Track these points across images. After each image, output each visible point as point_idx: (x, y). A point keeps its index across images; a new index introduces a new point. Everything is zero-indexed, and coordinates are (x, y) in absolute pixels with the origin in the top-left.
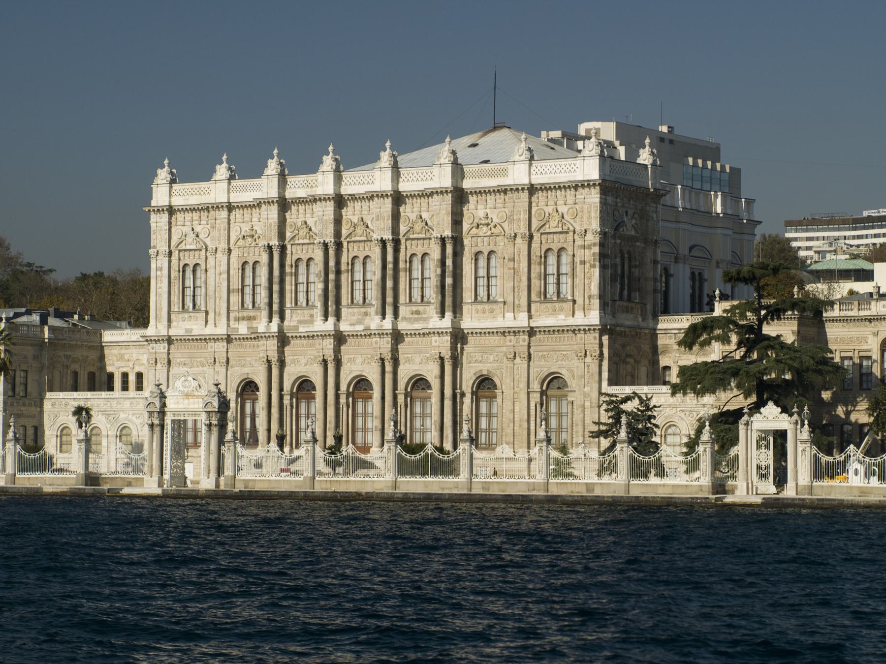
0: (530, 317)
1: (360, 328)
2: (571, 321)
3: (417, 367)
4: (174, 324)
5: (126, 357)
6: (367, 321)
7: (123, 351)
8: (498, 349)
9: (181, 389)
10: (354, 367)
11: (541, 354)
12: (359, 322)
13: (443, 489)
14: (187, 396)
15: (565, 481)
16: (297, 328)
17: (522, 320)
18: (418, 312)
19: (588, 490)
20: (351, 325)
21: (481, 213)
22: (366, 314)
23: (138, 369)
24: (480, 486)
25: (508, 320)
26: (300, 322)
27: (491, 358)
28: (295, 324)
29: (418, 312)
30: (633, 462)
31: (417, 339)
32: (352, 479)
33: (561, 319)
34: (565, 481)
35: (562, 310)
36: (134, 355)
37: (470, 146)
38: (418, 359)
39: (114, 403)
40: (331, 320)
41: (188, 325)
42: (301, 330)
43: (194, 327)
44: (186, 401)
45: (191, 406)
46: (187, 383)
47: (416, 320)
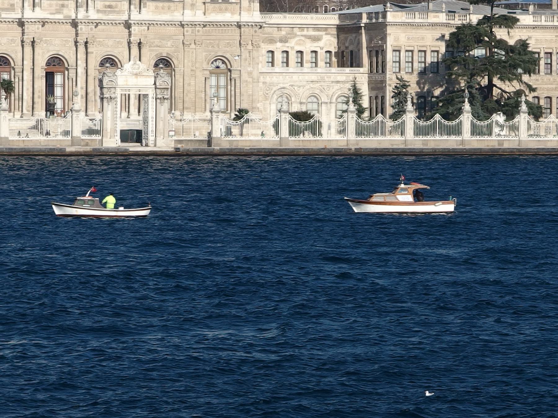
1: (60, 16)
2: (236, 18)
3: (109, 49)
6: (65, 11)
8: (175, 37)
9: (130, 70)
10: (51, 48)
11: (208, 41)
12: (58, 12)
13: (392, 145)
15: (481, 138)
17: (199, 17)
19: (499, 145)
20: (51, 14)
22: (63, 6)
24: (421, 142)
25: (189, 16)
27: (169, 44)
29: (110, 7)
30: (473, 125)
31: (110, 27)
32: (318, 138)
34: (481, 138)
35: (226, 9)
38: (110, 42)
40: (37, 9)
46: (137, 67)
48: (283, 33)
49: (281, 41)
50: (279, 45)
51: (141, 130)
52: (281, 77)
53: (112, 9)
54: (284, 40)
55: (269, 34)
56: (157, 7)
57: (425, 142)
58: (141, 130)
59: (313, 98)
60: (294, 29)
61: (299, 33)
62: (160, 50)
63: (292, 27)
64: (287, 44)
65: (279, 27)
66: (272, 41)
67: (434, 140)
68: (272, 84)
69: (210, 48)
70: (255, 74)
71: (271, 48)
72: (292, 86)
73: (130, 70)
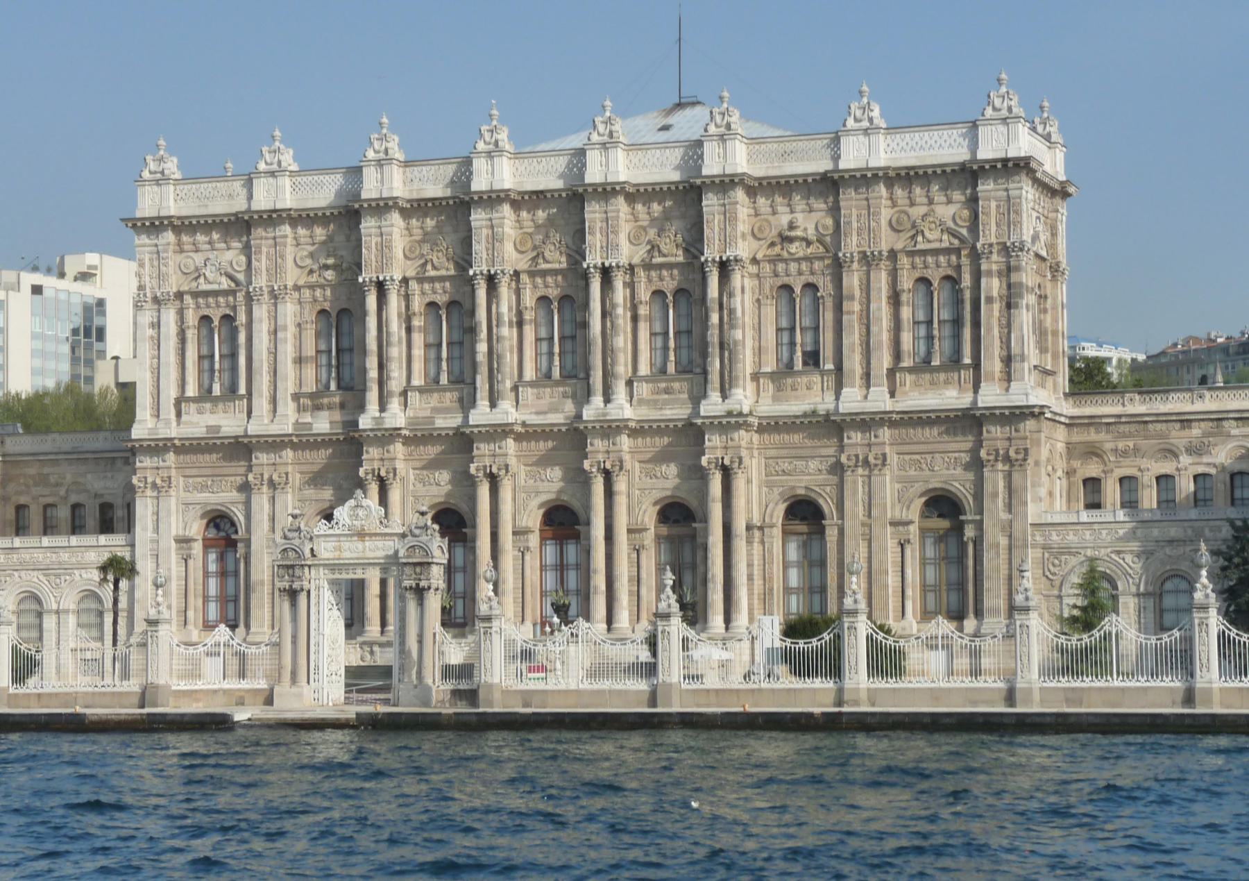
0: (892, 394)
4: (184, 418)
5: (52, 480)
7: (46, 470)
12: (554, 409)
14: (362, 535)
16: (430, 420)
17: (879, 400)
18: (667, 391)
20: (538, 413)
21: (785, 220)
23: (74, 498)
26: (435, 410)
28: (428, 413)
33: (952, 397)
35: (947, 382)
36: (69, 477)
37: (660, 129)
39: (65, 556)
40: (506, 405)
41: (210, 419)
42: (440, 422)
43: (223, 423)
44: (360, 545)
45: (369, 554)
46: (361, 512)
47: (666, 403)
48: (1196, 431)
49: (1190, 451)
50: (1185, 460)
51: (391, 667)
52: (1088, 533)
53: (673, 397)
54: (1195, 450)
55: (1161, 436)
56: (779, 389)
57: (1073, 695)
58: (391, 667)
59: (1176, 581)
60: (1225, 423)
61: (1234, 432)
62: (791, 481)
63: (1218, 419)
64: (1206, 459)
65: (1185, 421)
66: (1172, 453)
67: (1100, 689)
68: (1068, 551)
69: (912, 473)
70: (1017, 527)
71: (1167, 468)
72: (1118, 553)
73: (348, 521)
